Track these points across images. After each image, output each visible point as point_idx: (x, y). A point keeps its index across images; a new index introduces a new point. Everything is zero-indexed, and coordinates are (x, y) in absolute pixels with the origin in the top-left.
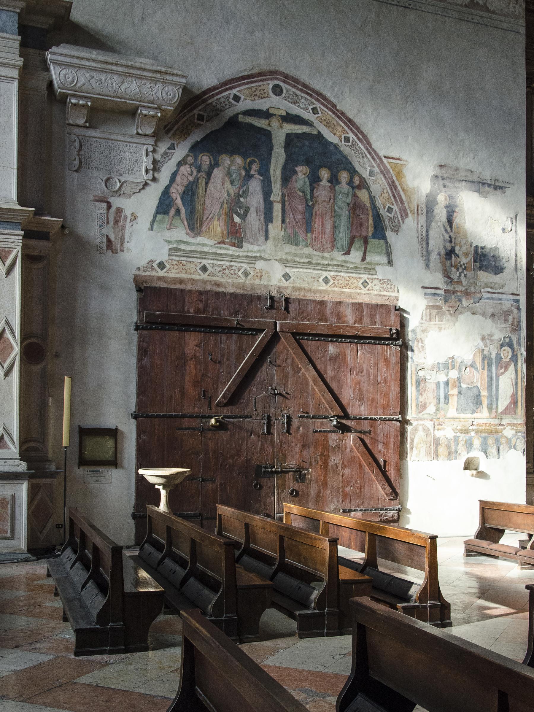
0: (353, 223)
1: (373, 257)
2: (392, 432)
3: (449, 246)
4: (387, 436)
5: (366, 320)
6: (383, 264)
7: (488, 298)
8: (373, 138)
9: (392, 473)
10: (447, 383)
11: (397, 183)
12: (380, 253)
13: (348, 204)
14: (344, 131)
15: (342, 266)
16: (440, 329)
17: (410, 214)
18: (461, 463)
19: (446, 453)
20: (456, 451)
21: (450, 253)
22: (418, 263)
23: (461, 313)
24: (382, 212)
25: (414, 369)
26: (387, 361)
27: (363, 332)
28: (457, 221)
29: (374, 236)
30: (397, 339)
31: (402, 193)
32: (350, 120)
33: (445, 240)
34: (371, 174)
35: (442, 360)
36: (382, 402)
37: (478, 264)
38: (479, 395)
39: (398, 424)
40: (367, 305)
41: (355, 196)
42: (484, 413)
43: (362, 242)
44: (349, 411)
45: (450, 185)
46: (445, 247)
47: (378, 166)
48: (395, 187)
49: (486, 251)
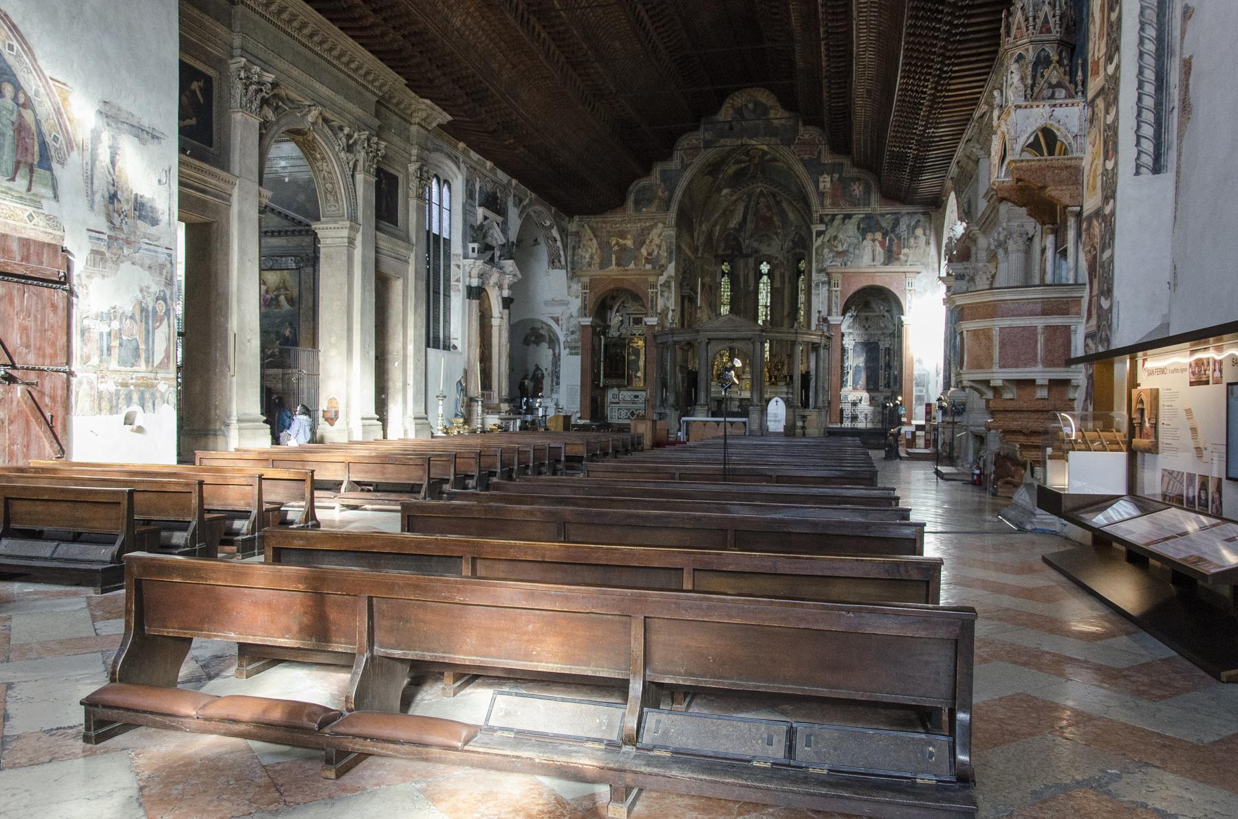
0: (18, 146)
1: (40, 189)
2: (59, 384)
3: (112, 190)
4: (54, 388)
5: (33, 258)
6: (48, 198)
7: (146, 249)
8: (38, 53)
9: (58, 429)
10: (109, 334)
11: (63, 110)
12: (45, 185)
13: (13, 123)
14: (8, 37)
15: (6, 193)
16: (104, 276)
17: (75, 148)
18: (121, 417)
19: (108, 407)
20: (117, 405)
21: (113, 197)
22: (83, 203)
23: (122, 262)
24: (49, 140)
25: (79, 317)
26: (54, 307)
27: (31, 272)
28: (119, 164)
29: (40, 166)
30: (64, 283)
31: (68, 123)
32: (14, 26)
33: (108, 183)
34: (37, 94)
35: (105, 310)
36: (49, 351)
37: (137, 213)
38: (137, 348)
39: (65, 375)
40: (35, 241)
41: (20, 116)
42: (142, 366)
43: (27, 170)
44: (16, 360)
45: (113, 124)
46: (108, 190)
47: (44, 87)
48: (61, 114)
49: (144, 200)
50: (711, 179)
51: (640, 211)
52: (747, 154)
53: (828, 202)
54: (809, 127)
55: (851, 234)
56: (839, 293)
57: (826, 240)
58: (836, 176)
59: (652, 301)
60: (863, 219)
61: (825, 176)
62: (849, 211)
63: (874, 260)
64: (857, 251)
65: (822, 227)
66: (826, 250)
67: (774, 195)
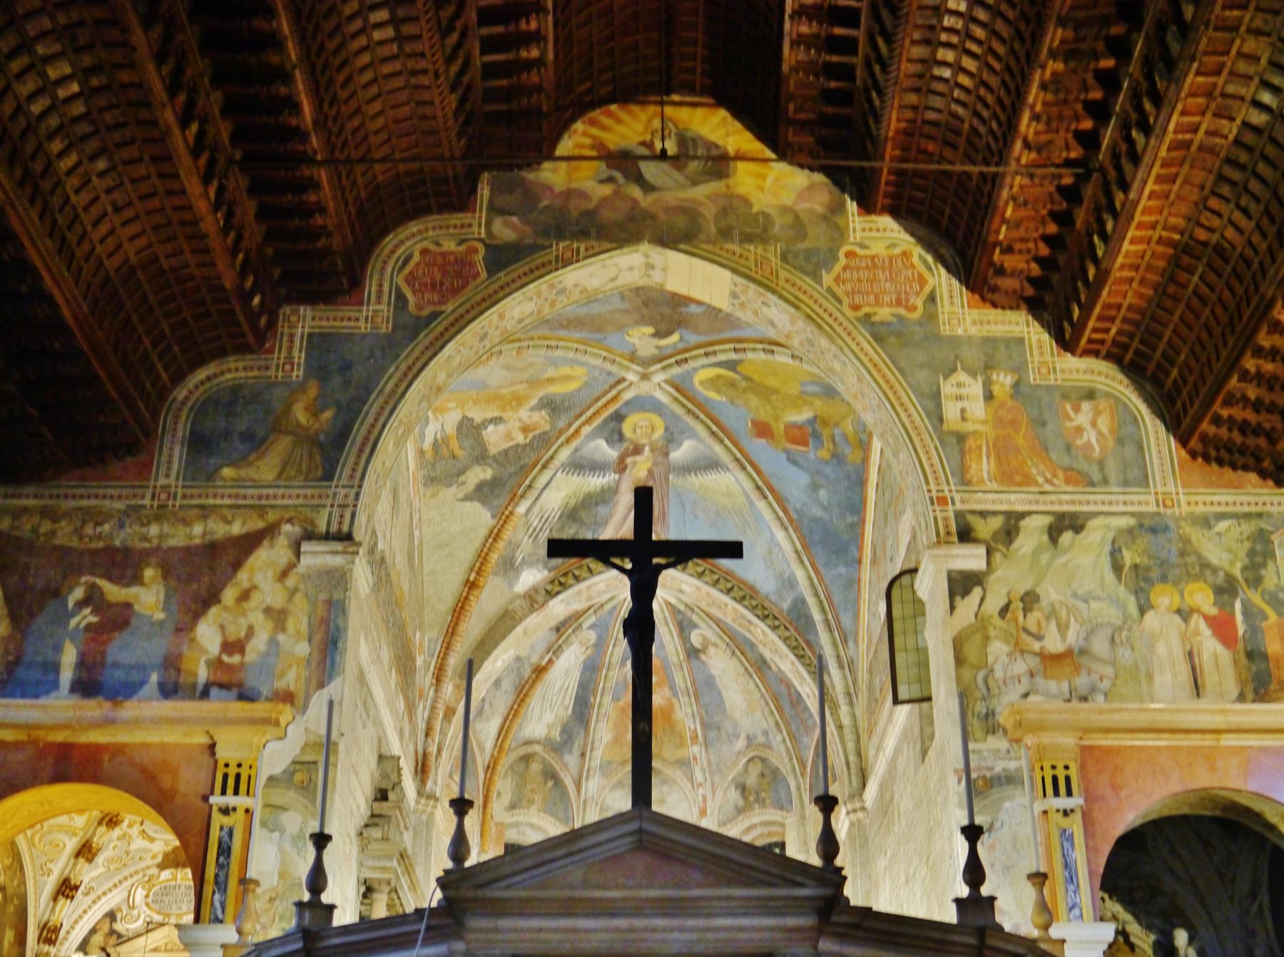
50: (480, 517)
51: (211, 477)
52: (616, 436)
53: (983, 467)
54: (886, 221)
55: (1087, 584)
56: (1078, 817)
57: (994, 604)
58: (1003, 381)
59: (225, 850)
60: (1130, 531)
61: (961, 376)
62: (1069, 501)
63: (1197, 689)
64: (1125, 655)
65: (970, 558)
66: (998, 649)
67: (684, 627)
